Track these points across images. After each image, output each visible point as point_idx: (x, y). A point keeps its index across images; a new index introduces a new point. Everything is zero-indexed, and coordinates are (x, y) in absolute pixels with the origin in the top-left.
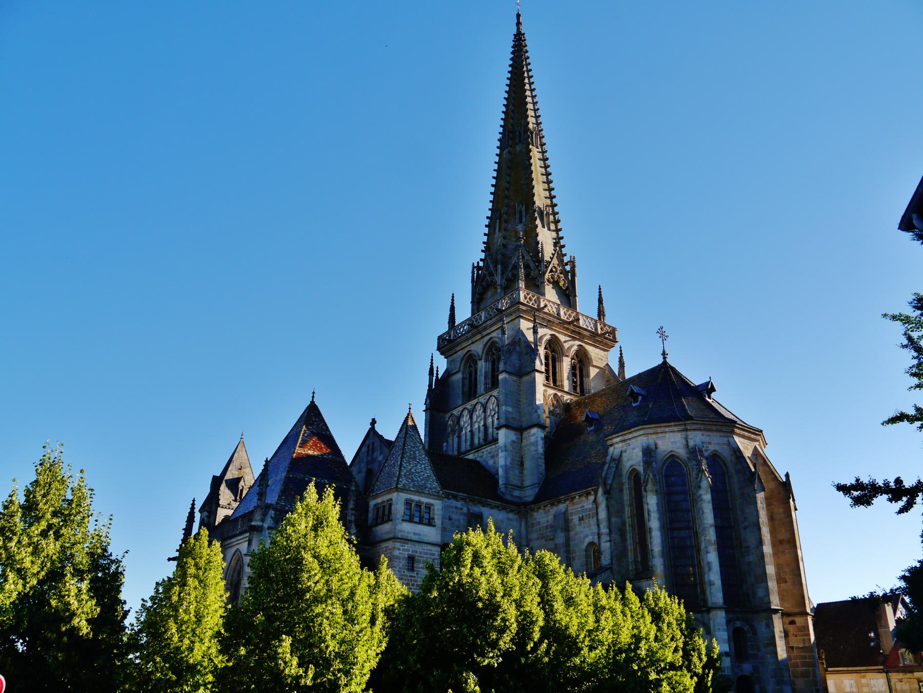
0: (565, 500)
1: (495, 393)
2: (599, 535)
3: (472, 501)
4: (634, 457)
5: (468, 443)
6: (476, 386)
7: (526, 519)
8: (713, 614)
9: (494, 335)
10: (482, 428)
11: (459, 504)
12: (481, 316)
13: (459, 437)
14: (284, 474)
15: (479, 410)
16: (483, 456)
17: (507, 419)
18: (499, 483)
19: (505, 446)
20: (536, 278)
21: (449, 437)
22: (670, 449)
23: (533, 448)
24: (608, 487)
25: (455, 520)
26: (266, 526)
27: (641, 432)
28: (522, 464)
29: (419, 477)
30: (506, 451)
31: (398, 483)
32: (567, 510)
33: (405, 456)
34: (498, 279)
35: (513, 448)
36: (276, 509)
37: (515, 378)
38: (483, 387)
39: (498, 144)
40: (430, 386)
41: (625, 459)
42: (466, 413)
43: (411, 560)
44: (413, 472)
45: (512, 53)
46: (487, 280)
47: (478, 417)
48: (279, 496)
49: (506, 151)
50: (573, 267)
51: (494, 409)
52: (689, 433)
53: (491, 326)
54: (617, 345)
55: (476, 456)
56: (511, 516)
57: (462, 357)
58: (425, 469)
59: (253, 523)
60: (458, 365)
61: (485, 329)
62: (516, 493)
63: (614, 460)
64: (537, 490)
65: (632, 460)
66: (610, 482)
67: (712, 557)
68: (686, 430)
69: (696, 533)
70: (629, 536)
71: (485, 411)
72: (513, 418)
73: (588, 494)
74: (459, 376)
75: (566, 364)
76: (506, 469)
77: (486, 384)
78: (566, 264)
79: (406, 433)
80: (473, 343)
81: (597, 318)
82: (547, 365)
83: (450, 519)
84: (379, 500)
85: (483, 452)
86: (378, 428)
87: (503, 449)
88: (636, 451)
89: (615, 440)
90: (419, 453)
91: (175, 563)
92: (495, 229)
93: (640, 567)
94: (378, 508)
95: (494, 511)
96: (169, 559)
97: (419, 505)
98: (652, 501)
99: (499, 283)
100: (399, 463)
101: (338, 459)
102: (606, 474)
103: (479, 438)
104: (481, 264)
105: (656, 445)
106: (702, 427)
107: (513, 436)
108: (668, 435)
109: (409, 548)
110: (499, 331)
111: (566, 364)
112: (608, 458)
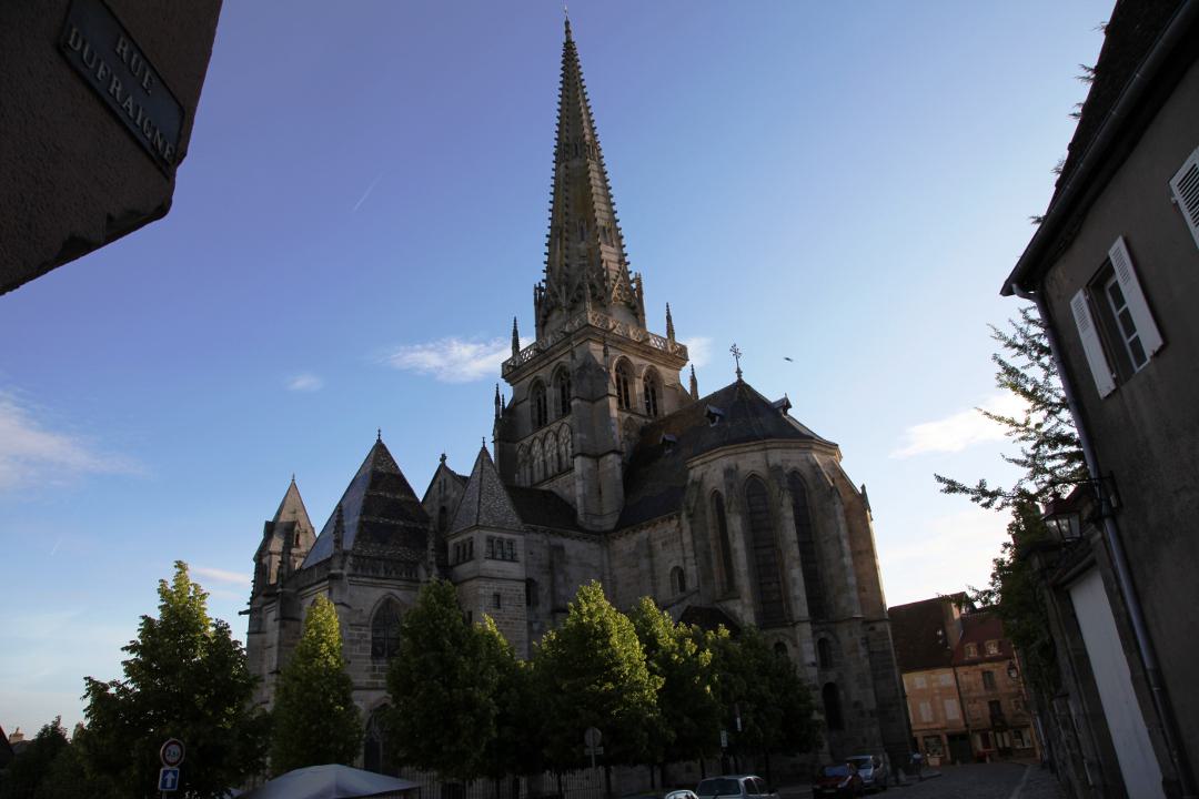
0: (648, 526)
1: (567, 420)
2: (685, 559)
3: (552, 532)
5: (542, 473)
6: (546, 412)
7: (608, 547)
8: (798, 628)
9: (562, 359)
10: (555, 457)
11: (539, 537)
13: (531, 467)
14: (357, 518)
15: (551, 439)
16: (558, 486)
22: (750, 469)
23: (610, 475)
26: (345, 573)
27: (722, 453)
28: (600, 492)
31: (478, 521)
32: (650, 536)
34: (563, 300)
36: (353, 555)
37: (588, 404)
38: (553, 413)
39: (554, 158)
40: (497, 416)
41: (707, 478)
42: (537, 442)
43: (497, 597)
45: (563, 62)
47: (550, 446)
48: (355, 541)
49: (563, 165)
50: (639, 285)
51: (566, 437)
52: (769, 451)
53: (559, 350)
54: (689, 364)
56: (592, 545)
59: (333, 571)
61: (553, 353)
62: (596, 522)
64: (617, 518)
66: (692, 504)
67: (796, 573)
68: (767, 449)
69: (780, 551)
70: (714, 558)
71: (557, 440)
73: (671, 518)
74: (528, 403)
75: (638, 387)
77: (556, 411)
78: (632, 282)
80: (540, 368)
81: (666, 337)
82: (619, 388)
84: (459, 539)
86: (448, 463)
89: (695, 463)
91: (248, 616)
92: (556, 249)
93: (725, 587)
94: (458, 548)
95: (576, 542)
96: (240, 613)
97: (500, 541)
98: (736, 523)
101: (411, 499)
103: (553, 468)
104: (543, 285)
105: (737, 466)
106: (781, 445)
107: (589, 463)
108: (748, 455)
109: (494, 587)
110: (569, 354)
111: (638, 387)
112: (690, 481)
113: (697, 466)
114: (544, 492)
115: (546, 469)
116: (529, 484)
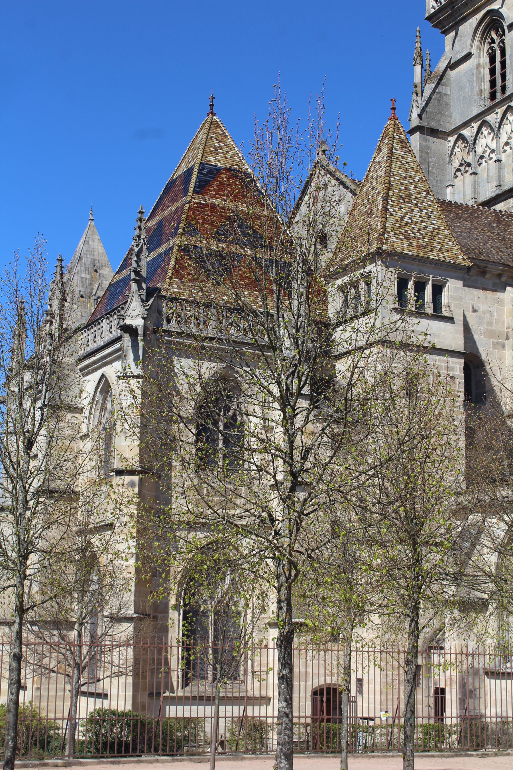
6: (504, 77)
21: (456, 177)
25: (484, 313)
29: (420, 230)
33: (391, 193)
44: (407, 224)
55: (511, 205)
57: (474, 26)
58: (429, 217)
59: (128, 322)
60: (469, 42)
79: (391, 153)
83: (475, 311)
90: (416, 187)
100: (380, 207)
114: (499, 215)
115: (500, 177)
116: (470, 203)
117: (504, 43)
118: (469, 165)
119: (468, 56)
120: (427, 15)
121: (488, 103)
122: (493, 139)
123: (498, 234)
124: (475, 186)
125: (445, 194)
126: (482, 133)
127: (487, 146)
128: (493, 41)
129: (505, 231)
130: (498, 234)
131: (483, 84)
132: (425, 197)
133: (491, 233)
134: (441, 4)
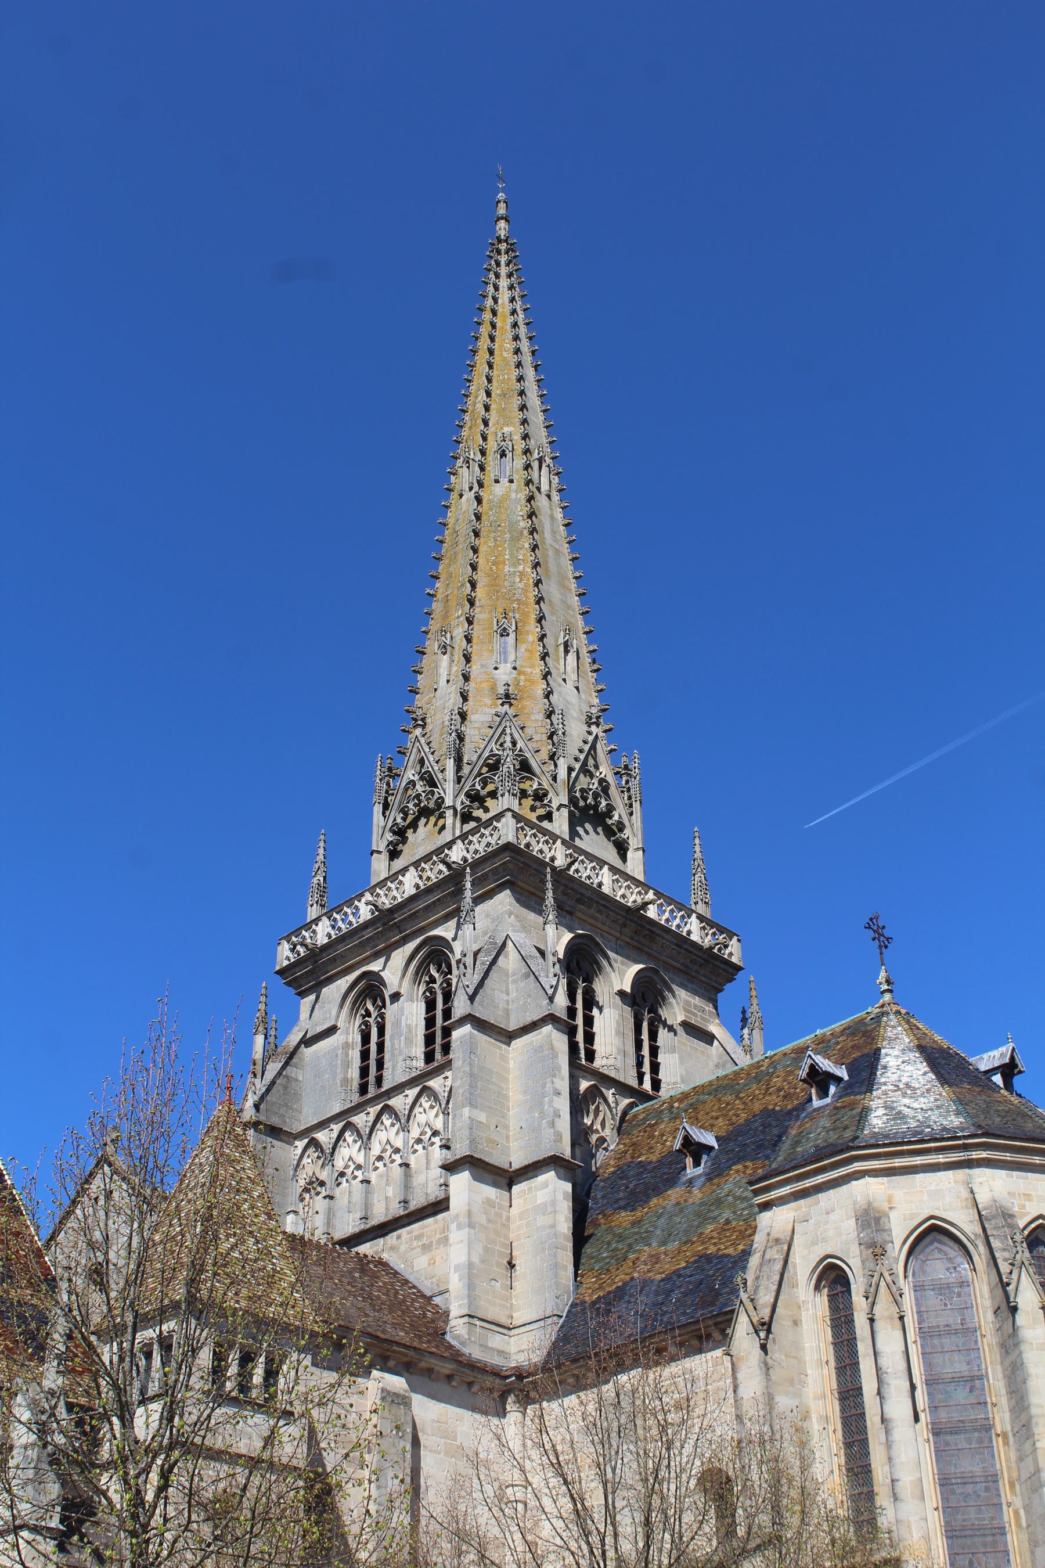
4: (831, 1233)
12: (400, 883)
17: (473, 1141)
18: (447, 1313)
19: (470, 1213)
20: (545, 795)
24: (766, 1313)
28: (511, 1265)
30: (471, 1225)
35: (489, 1221)
38: (401, 1065)
46: (418, 796)
57: (343, 990)
60: (334, 1012)
61: (414, 916)
63: (777, 1241)
65: (824, 1240)
68: (969, 1164)
72: (490, 1141)
76: (471, 1275)
85: (399, 1237)
87: (464, 1220)
88: (833, 1217)
90: (252, 1207)
99: (448, 801)
102: (757, 1278)
105: (890, 1200)
113: (783, 1201)
114: (363, 1261)
115: (367, 1205)
117: (383, 1018)
118: (322, 1184)
119: (332, 1030)
120: (278, 968)
121: (356, 1098)
122: (359, 1150)
123: (362, 1289)
124: (330, 1214)
125: (285, 1224)
126: (345, 1140)
127: (350, 1159)
128: (368, 1014)
129: (372, 1285)
130: (362, 1289)
131: (350, 1070)
132: (264, 1223)
133: (352, 1286)
134: (299, 955)
